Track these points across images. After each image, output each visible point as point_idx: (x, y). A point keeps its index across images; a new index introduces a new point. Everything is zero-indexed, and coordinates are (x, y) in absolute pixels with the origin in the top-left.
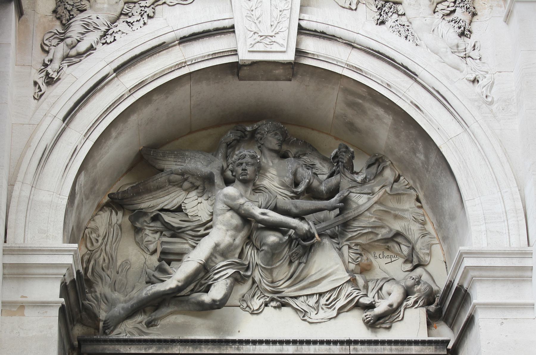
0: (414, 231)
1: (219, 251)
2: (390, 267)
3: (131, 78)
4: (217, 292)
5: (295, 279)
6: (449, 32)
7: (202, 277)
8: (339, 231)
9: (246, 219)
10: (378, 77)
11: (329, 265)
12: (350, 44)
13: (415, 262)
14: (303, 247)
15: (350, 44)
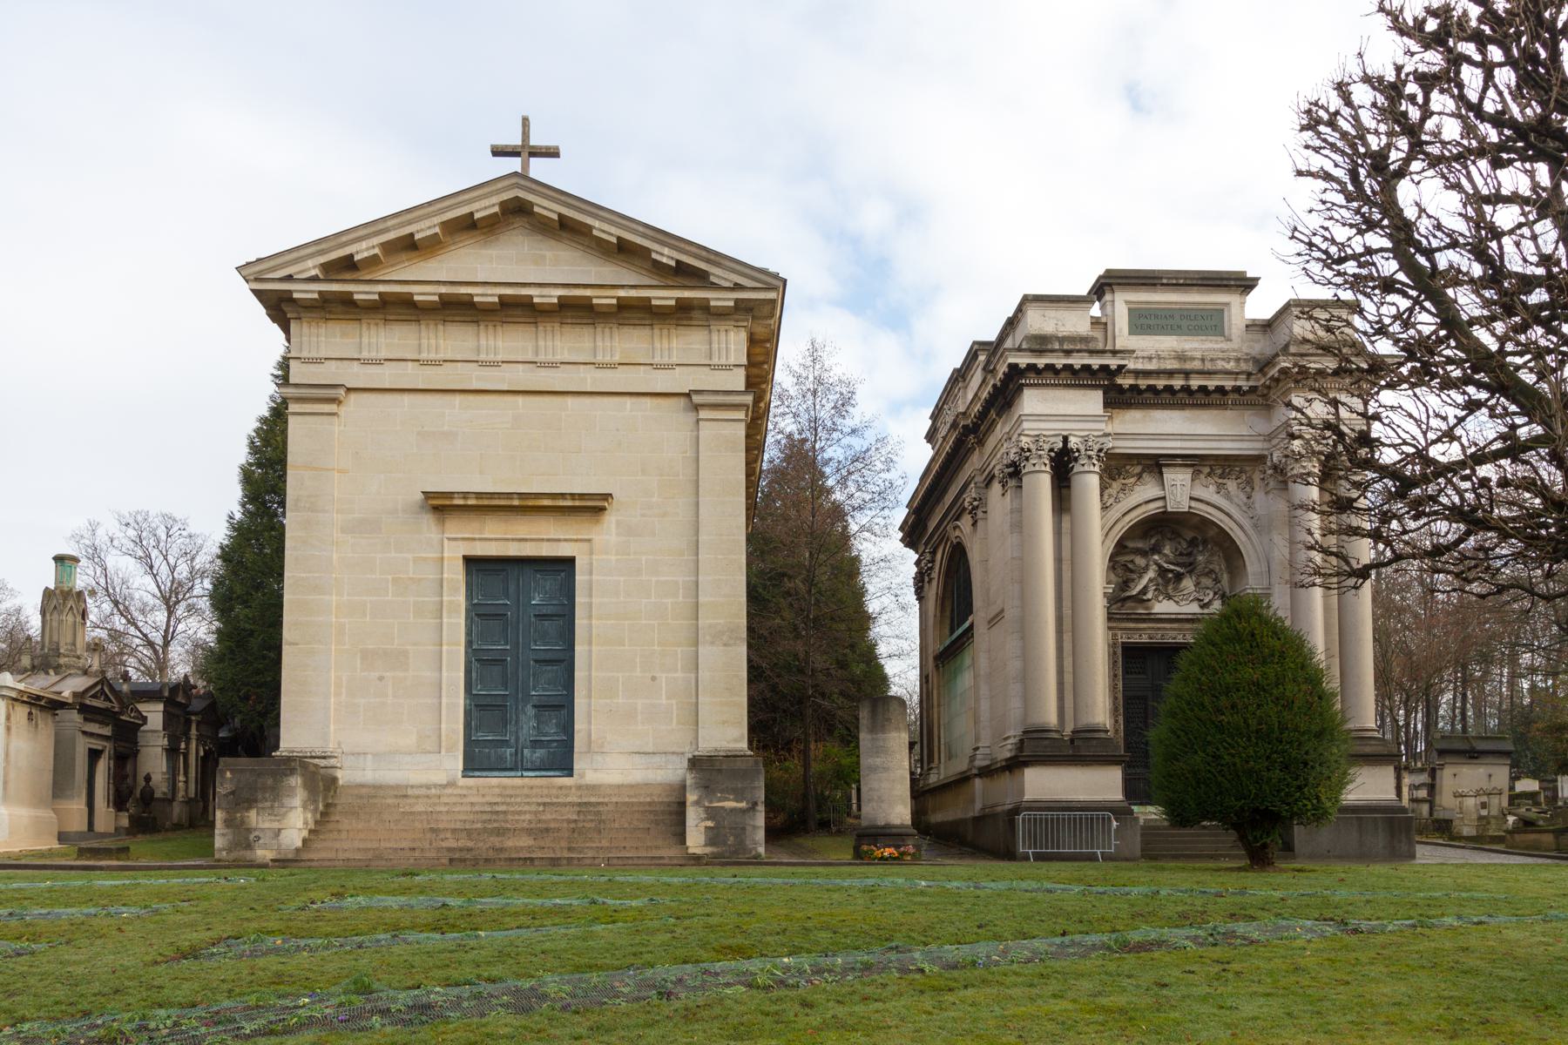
0: (1217, 569)
1: (1151, 580)
2: (1207, 582)
3: (1127, 518)
4: (1149, 596)
5: (1175, 589)
6: (1243, 497)
7: (1144, 591)
8: (1190, 572)
9: (1160, 566)
10: (1216, 516)
11: (1188, 584)
12: (1208, 504)
13: (1217, 581)
14: (1179, 577)
15: (1208, 504)
